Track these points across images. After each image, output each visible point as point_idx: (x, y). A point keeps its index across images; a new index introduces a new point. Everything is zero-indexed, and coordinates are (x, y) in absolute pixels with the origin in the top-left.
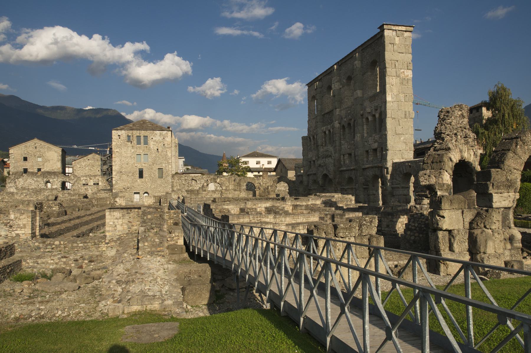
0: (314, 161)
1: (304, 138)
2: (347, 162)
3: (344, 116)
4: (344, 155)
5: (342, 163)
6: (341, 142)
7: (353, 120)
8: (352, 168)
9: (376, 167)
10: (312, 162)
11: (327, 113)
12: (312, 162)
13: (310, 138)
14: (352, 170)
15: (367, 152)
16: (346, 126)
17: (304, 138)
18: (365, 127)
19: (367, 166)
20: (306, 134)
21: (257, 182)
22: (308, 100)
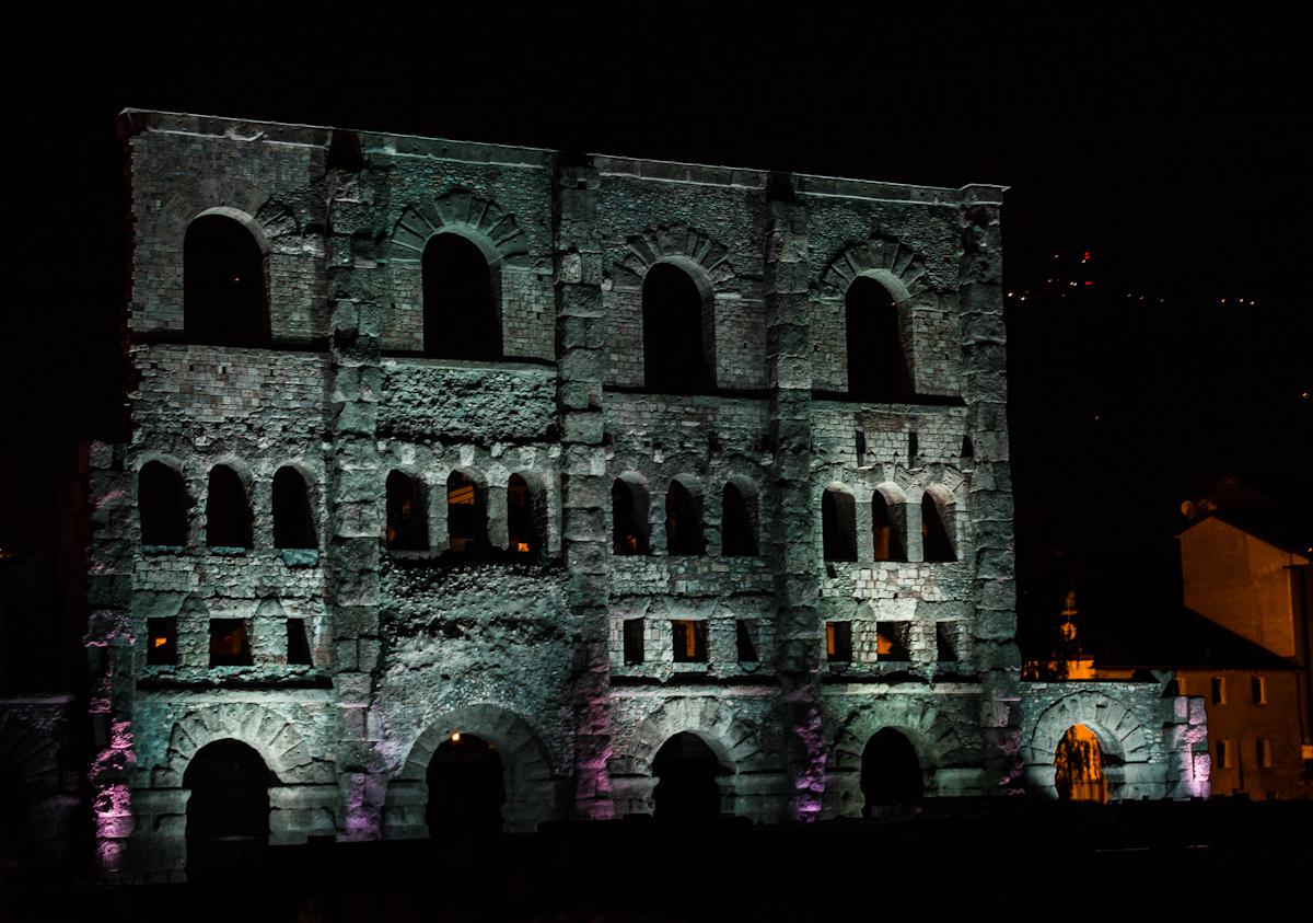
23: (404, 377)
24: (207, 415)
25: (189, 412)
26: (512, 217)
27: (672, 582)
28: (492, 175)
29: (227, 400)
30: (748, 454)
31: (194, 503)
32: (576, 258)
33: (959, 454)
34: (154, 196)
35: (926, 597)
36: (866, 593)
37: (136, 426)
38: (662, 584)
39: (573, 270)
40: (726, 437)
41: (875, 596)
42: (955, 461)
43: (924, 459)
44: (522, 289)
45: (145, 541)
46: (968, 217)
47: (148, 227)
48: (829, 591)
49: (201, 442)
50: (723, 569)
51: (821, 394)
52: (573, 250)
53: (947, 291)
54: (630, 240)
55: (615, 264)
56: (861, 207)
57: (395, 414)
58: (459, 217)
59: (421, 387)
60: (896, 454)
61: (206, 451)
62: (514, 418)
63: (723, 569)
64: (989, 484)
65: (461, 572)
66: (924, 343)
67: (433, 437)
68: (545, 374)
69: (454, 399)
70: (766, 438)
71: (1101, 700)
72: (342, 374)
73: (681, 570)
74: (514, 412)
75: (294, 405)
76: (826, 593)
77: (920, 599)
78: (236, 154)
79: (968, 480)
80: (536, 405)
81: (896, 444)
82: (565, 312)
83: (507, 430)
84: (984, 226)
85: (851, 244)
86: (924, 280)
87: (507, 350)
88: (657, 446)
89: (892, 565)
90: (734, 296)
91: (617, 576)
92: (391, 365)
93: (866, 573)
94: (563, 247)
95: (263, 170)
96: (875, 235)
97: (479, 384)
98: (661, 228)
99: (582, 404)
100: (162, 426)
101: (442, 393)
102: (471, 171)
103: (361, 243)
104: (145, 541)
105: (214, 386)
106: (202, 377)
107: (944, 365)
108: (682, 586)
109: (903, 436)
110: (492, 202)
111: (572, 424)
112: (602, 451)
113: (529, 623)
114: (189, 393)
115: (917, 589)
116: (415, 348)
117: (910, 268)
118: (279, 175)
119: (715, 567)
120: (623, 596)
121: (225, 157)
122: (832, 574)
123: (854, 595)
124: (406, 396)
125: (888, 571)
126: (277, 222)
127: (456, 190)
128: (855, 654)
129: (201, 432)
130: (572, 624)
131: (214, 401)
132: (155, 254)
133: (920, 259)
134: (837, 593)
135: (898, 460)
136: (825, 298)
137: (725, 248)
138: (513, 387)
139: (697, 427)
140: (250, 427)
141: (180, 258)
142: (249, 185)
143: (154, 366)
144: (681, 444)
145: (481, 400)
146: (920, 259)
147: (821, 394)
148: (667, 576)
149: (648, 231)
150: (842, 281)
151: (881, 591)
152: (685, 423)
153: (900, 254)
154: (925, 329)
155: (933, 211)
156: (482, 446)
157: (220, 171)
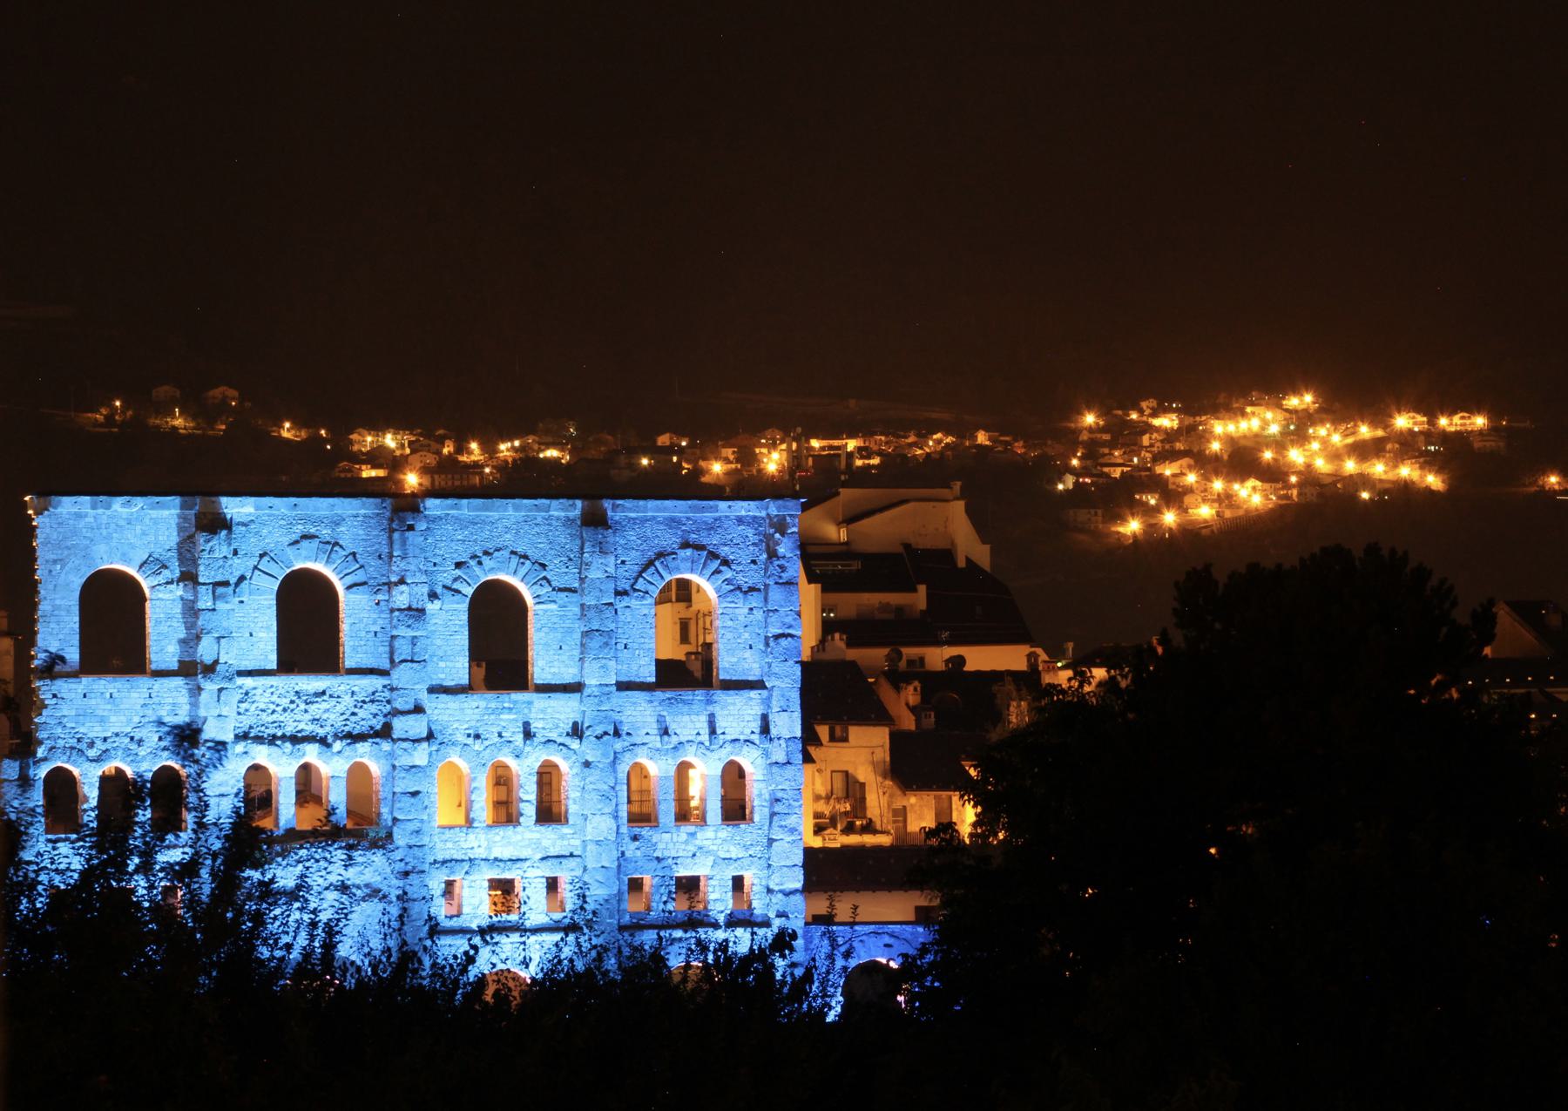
23: (259, 692)
24: (93, 730)
25: (82, 730)
26: (354, 554)
27: (489, 848)
28: (337, 522)
29: (113, 719)
30: (559, 740)
31: (86, 799)
32: (403, 588)
33: (757, 730)
34: (55, 562)
36: (666, 854)
37: (40, 743)
38: (481, 850)
39: (402, 597)
40: (540, 724)
42: (755, 738)
44: (357, 617)
45: (47, 832)
46: (771, 525)
47: (51, 587)
49: (92, 753)
50: (537, 835)
51: (623, 686)
52: (402, 581)
53: (752, 589)
54: (458, 565)
55: (445, 587)
56: (673, 522)
57: (252, 721)
58: (307, 558)
59: (274, 698)
61: (97, 760)
62: (353, 719)
63: (537, 835)
64: (782, 758)
65: (302, 847)
66: (729, 635)
67: (284, 738)
68: (377, 682)
69: (303, 706)
70: (575, 724)
71: (887, 940)
72: (204, 695)
73: (498, 838)
74: (354, 714)
76: (628, 854)
78: (122, 523)
79: (766, 754)
80: (373, 708)
81: (698, 725)
82: (395, 633)
83: (347, 729)
84: (783, 534)
85: (660, 555)
86: (728, 581)
87: (349, 662)
88: (477, 736)
89: (691, 829)
90: (553, 606)
92: (248, 682)
94: (394, 579)
95: (144, 534)
96: (686, 545)
97: (324, 693)
98: (486, 553)
99: (411, 706)
100: (61, 743)
101: (292, 702)
102: (319, 521)
103: (220, 590)
104: (47, 832)
105: (103, 708)
106: (93, 702)
107: (748, 654)
108: (496, 853)
109: (704, 718)
110: (337, 544)
111: (400, 726)
112: (425, 745)
113: (358, 887)
114: (82, 715)
116: (269, 667)
117: (717, 572)
118: (156, 536)
119: (528, 835)
120: (444, 862)
121: (113, 526)
122: (635, 838)
124: (262, 706)
126: (156, 573)
127: (305, 537)
129: (91, 745)
130: (393, 887)
131: (103, 720)
132: (55, 608)
133: (726, 563)
134: (638, 853)
135: (700, 738)
136: (634, 603)
137: (543, 566)
138: (353, 693)
140: (132, 738)
141: (76, 610)
142: (133, 547)
143: (55, 696)
144: (500, 735)
145: (325, 706)
146: (726, 563)
147: (623, 686)
149: (474, 557)
150: (651, 588)
153: (716, 559)
154: (730, 623)
155: (740, 520)
156: (323, 741)
157: (109, 538)
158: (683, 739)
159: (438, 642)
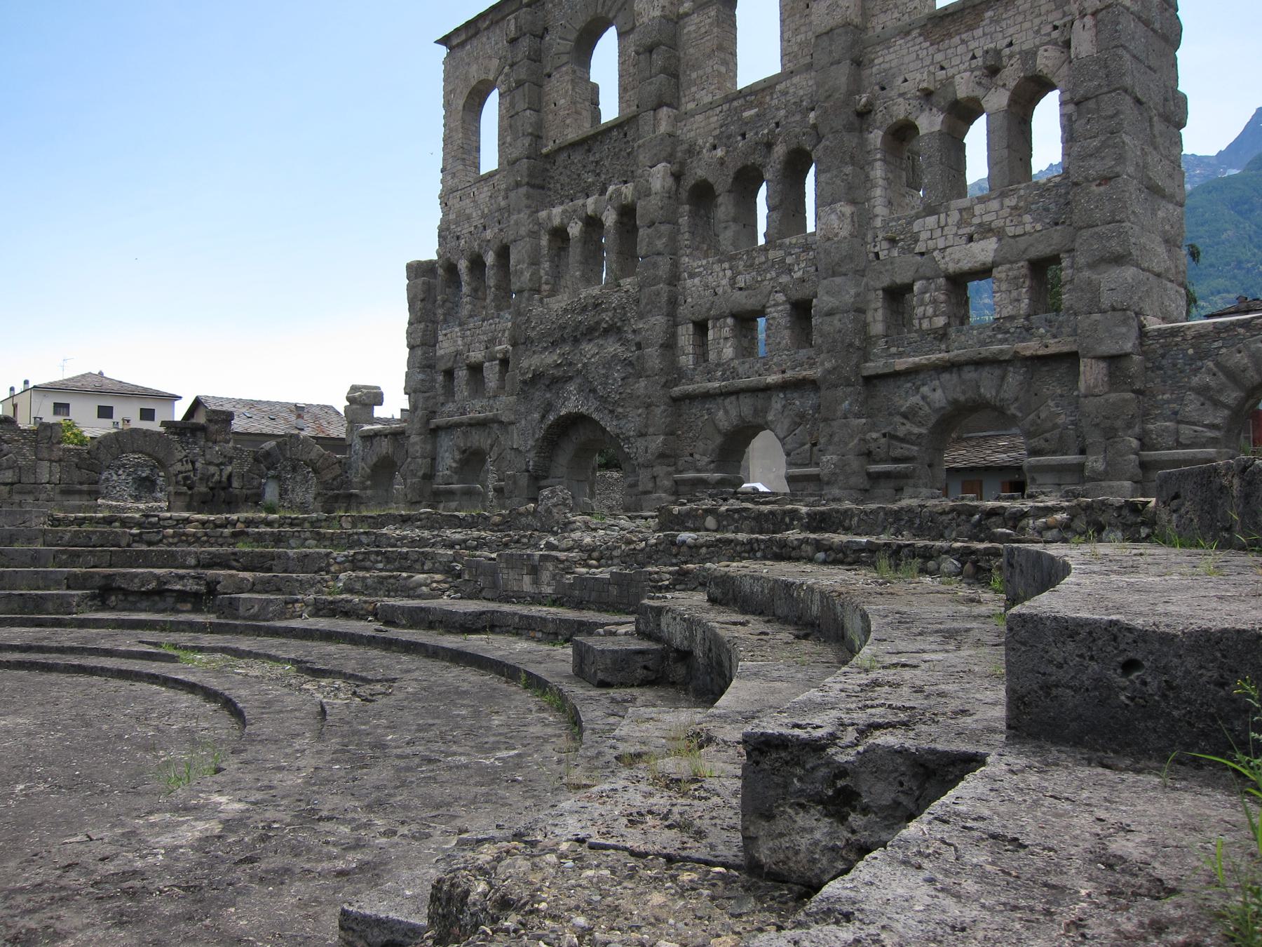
0: (476, 370)
1: (417, 271)
2: (728, 352)
3: (705, 142)
4: (701, 327)
5: (687, 360)
6: (675, 264)
7: (780, 150)
8: (772, 379)
9: (979, 363)
10: (462, 374)
11: (574, 145)
12: (462, 374)
13: (451, 269)
14: (767, 389)
15: (897, 295)
16: (722, 183)
17: (417, 271)
18: (878, 172)
19: (901, 364)
20: (428, 251)
21: (179, 455)
22: (447, 105)
35: (1010, 231)
41: (941, 244)
43: (1016, 48)
48: (886, 252)
60: (974, 57)
75: (503, 203)
77: (1000, 234)
81: (972, 45)
91: (689, 282)
93: (931, 221)
115: (1000, 223)
123: (917, 250)
125: (960, 211)
128: (916, 322)
139: (757, 115)
148: (729, 273)
151: (950, 237)
152: (746, 114)
158: (951, 72)
159: (692, 51)
